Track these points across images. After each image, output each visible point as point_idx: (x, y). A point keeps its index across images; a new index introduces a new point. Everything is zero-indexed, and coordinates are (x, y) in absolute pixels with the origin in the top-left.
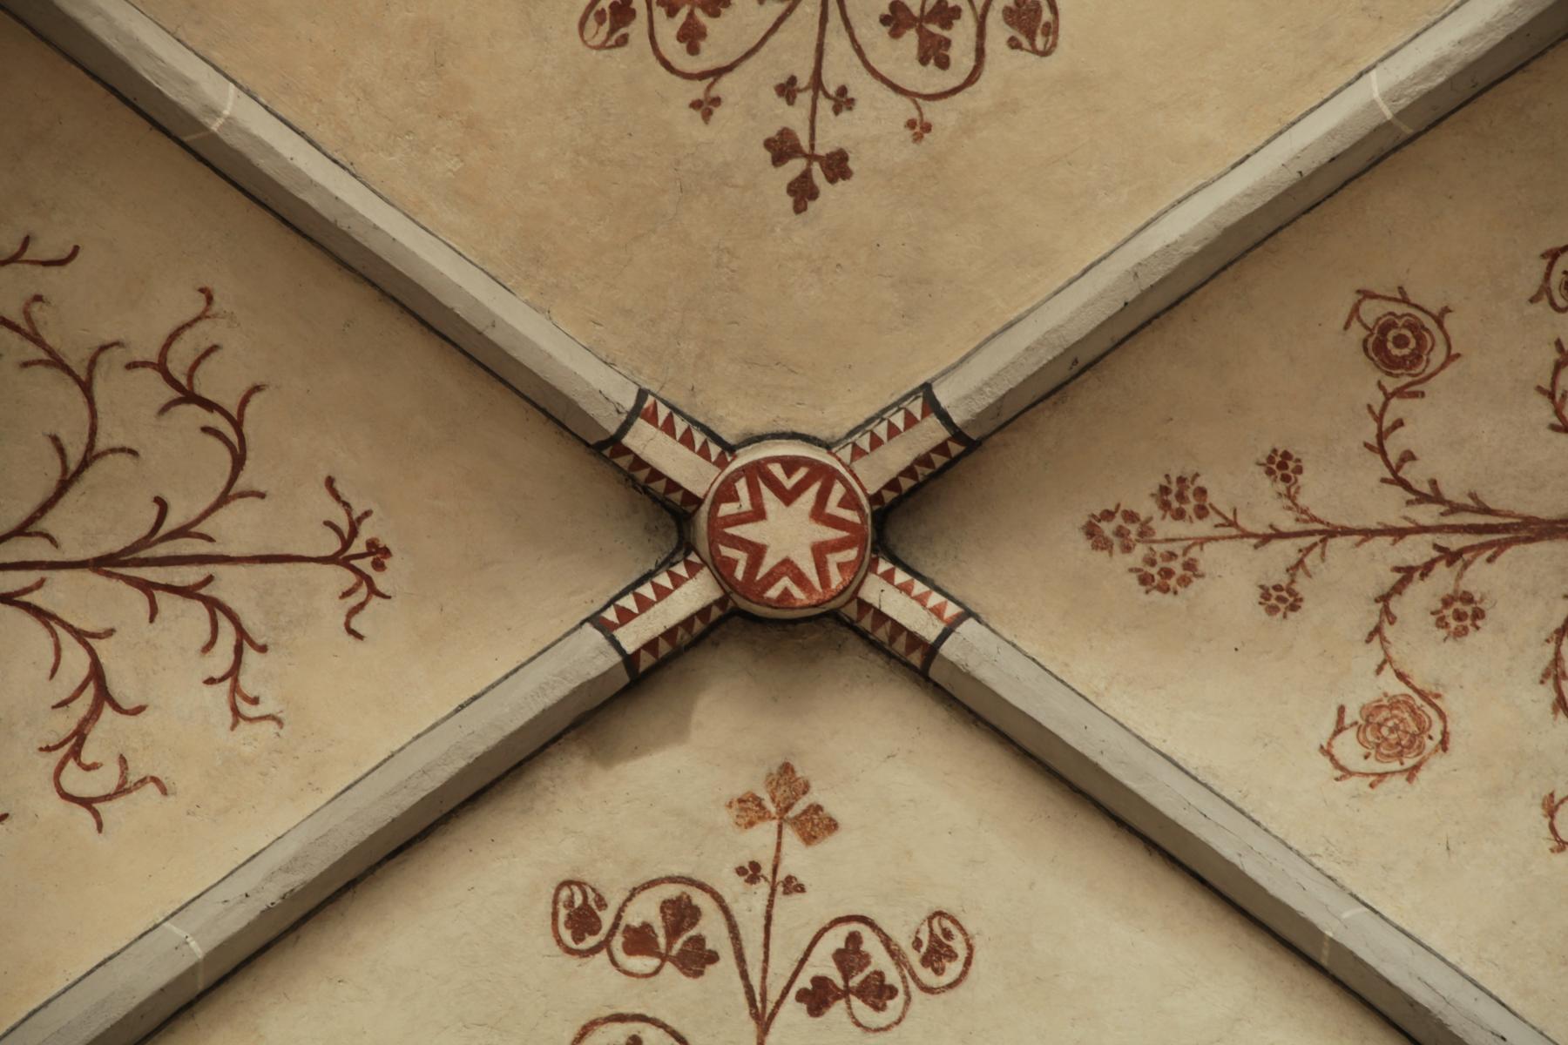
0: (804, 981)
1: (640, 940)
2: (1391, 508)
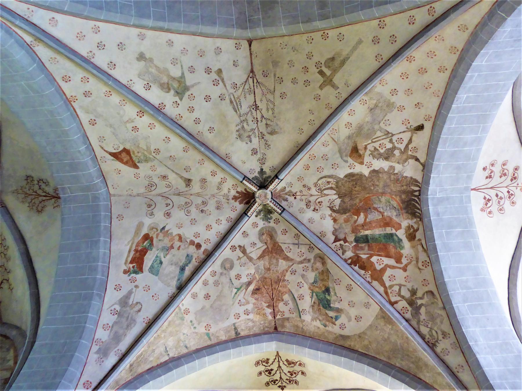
0: (510, 191)
1: (514, 175)
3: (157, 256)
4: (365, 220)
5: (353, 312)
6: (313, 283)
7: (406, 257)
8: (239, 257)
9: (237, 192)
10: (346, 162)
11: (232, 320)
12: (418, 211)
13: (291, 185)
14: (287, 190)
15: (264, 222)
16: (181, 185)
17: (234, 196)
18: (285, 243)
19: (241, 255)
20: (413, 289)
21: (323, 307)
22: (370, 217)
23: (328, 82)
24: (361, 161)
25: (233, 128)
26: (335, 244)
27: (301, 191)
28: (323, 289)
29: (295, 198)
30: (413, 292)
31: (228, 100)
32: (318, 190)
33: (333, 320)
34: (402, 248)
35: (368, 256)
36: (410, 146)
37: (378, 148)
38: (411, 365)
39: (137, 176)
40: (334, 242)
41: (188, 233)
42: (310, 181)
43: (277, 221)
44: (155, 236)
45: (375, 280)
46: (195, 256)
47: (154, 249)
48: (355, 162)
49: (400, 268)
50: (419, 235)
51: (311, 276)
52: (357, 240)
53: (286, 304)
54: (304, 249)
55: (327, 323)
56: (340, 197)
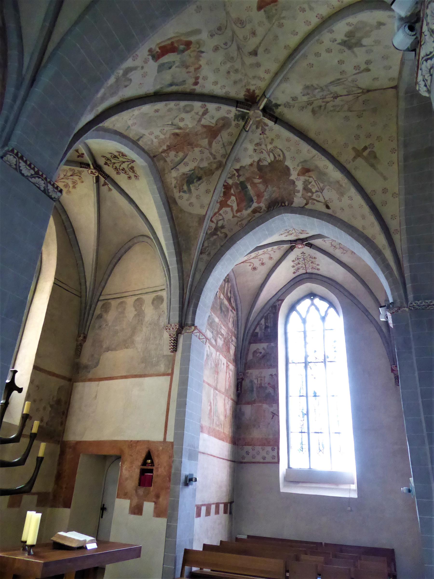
2: (269, 253)
3: (174, 62)
4: (258, 183)
5: (193, 200)
6: (200, 168)
7: (241, 214)
8: (198, 113)
9: (254, 91)
10: (298, 166)
11: (146, 132)
12: (272, 208)
13: (271, 130)
14: (266, 128)
15: (233, 117)
17: (250, 89)
18: (221, 138)
19: (200, 113)
20: (224, 226)
21: (187, 181)
23: (358, 154)
25: (315, 83)
26: (234, 170)
27: (267, 137)
28: (199, 175)
29: (261, 134)
30: (223, 227)
31: (340, 77)
32: (272, 150)
33: (181, 190)
34: (246, 209)
35: (234, 193)
36: (315, 201)
37: (312, 184)
38: (184, 246)
39: (249, 9)
40: (235, 170)
41: (206, 71)
42: (277, 143)
43: (237, 126)
44: (192, 49)
45: (220, 204)
46: (186, 86)
47: (179, 56)
49: (233, 214)
50: (257, 215)
51: (205, 164)
52: (242, 183)
53: (176, 156)
54: (222, 151)
55: (178, 187)
56: (269, 164)
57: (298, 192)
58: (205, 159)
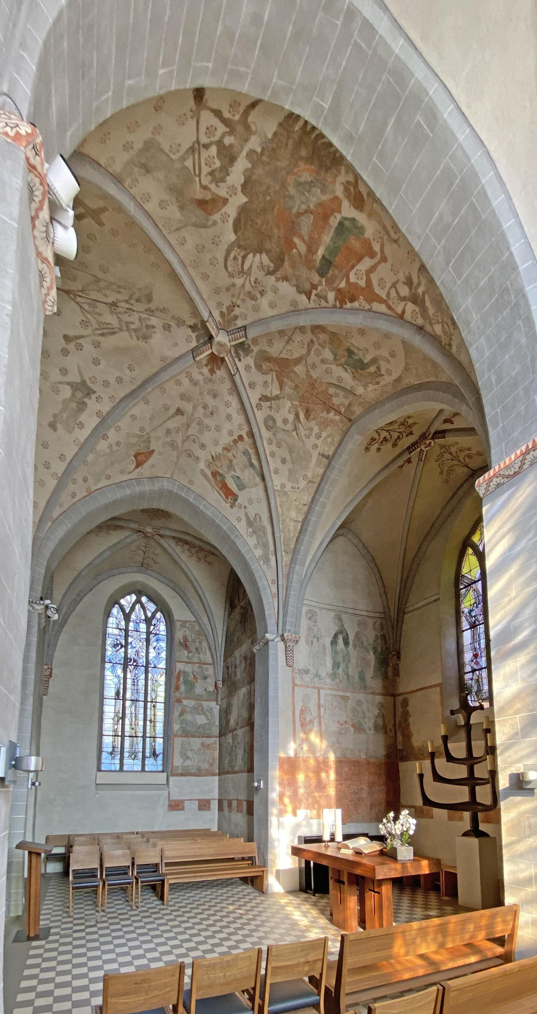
4: (303, 240)
10: (215, 223)
16: (180, 420)
22: (305, 231)
24: (222, 201)
26: (311, 301)
40: (309, 299)
48: (219, 210)
57: (252, 152)
58: (321, 357)
